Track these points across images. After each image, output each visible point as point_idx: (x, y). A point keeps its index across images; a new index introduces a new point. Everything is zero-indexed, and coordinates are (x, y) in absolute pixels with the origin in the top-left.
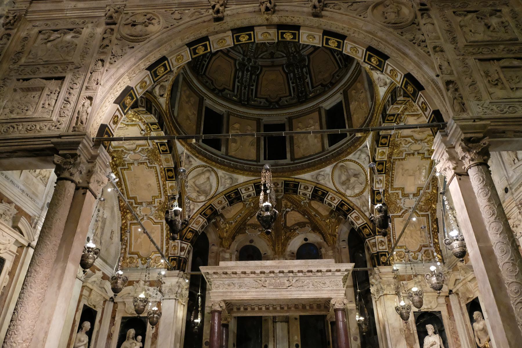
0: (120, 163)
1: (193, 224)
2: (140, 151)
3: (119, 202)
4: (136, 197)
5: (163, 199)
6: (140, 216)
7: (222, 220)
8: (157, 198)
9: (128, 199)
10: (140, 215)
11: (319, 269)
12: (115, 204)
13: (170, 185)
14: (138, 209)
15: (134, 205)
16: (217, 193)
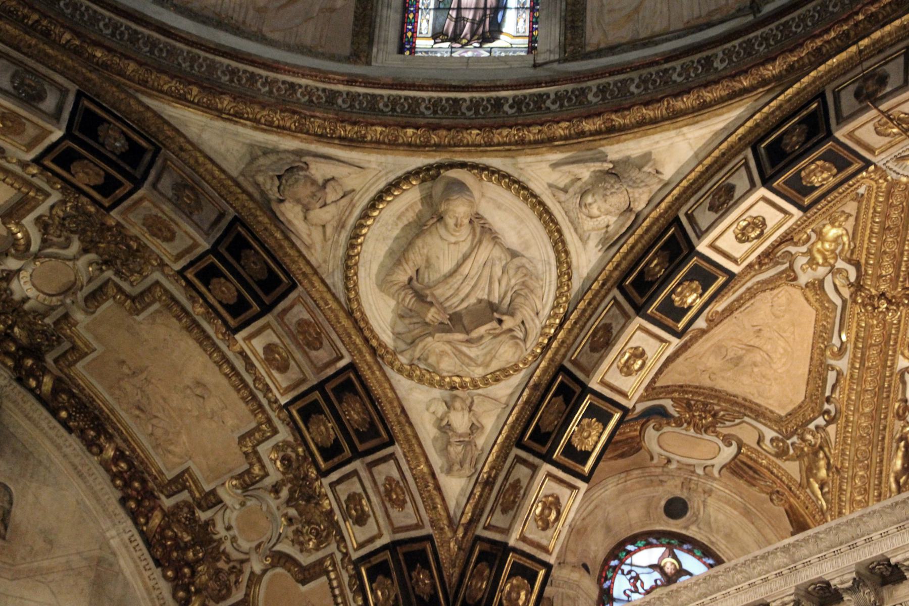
0: (31, 333)
1: (492, 511)
2: (45, 242)
3: (136, 523)
4: (187, 470)
5: (284, 434)
6: (242, 562)
7: (769, 434)
8: (260, 443)
9: (168, 497)
10: (242, 557)
11: (868, 553)
12: (114, 543)
13: (258, 344)
14: (220, 528)
15: (203, 516)
16: (576, 284)
